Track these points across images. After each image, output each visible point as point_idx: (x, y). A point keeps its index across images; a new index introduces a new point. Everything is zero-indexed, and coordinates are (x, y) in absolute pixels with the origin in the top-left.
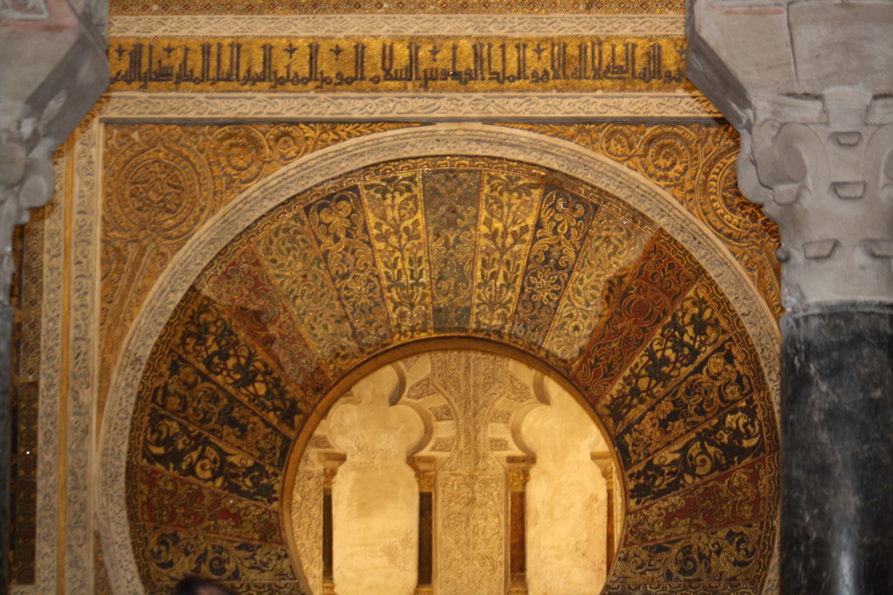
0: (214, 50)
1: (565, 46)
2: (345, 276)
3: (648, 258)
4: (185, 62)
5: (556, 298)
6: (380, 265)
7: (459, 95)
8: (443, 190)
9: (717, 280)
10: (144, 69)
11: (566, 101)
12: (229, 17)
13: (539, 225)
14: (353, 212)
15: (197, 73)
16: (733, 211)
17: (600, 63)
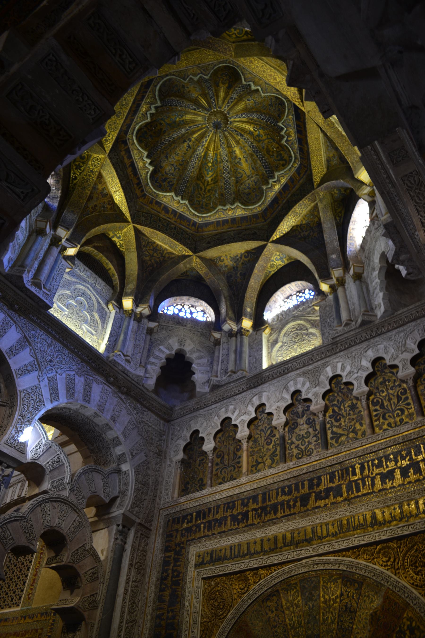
0: (233, 548)
1: (342, 521)
2: (275, 627)
3: (384, 602)
4: (225, 554)
5: (351, 626)
6: (287, 620)
7: (308, 548)
8: (307, 586)
9: (415, 607)
10: (214, 558)
11: (345, 542)
12: (238, 536)
13: (342, 594)
14: (278, 600)
15: (228, 557)
16: (417, 574)
17: (355, 524)
